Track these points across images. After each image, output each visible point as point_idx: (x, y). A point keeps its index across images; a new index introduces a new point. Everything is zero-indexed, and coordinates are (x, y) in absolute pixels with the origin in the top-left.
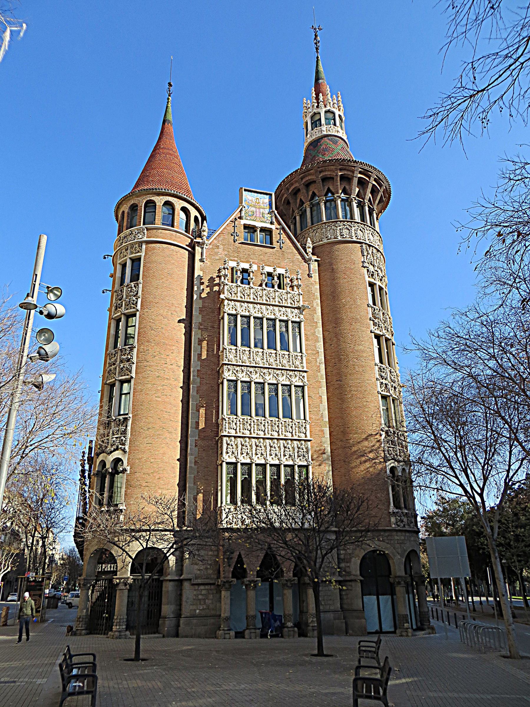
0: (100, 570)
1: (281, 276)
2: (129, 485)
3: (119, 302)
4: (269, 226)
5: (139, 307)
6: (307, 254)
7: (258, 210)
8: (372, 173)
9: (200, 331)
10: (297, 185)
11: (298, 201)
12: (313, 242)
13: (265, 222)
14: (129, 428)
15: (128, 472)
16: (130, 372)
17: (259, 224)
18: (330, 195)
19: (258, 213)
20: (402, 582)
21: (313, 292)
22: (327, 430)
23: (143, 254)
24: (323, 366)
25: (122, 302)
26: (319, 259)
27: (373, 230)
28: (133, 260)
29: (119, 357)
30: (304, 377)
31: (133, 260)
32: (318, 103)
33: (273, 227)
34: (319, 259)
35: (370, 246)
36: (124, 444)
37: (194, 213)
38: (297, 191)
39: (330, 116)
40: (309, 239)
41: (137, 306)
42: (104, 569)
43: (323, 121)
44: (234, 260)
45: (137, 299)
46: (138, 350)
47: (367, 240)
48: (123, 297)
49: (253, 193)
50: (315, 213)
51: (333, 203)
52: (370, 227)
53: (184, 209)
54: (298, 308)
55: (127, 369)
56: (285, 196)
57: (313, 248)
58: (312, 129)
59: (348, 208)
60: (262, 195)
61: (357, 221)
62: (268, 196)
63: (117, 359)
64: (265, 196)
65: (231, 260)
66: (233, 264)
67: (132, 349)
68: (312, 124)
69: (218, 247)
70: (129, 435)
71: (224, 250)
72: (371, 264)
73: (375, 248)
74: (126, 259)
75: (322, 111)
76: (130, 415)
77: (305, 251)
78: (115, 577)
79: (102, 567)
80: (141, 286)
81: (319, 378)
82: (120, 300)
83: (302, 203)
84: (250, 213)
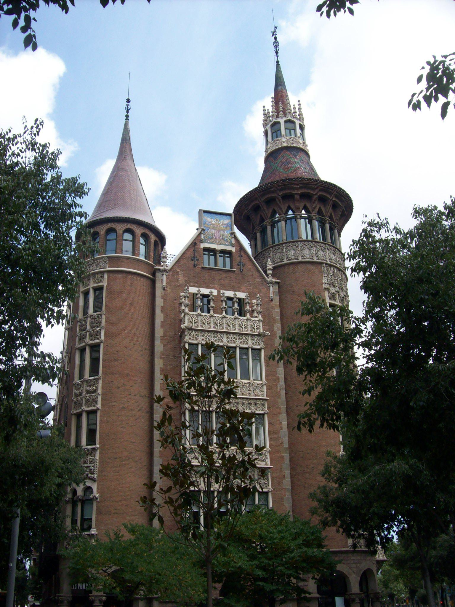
0: (76, 588)
1: (242, 300)
2: (99, 512)
3: (83, 333)
4: (229, 248)
5: (102, 337)
6: (267, 275)
7: (217, 232)
8: (332, 190)
10: (257, 202)
11: (259, 216)
12: (274, 262)
14: (97, 458)
15: (98, 500)
16: (96, 403)
18: (290, 212)
20: (357, 599)
21: (273, 316)
22: (287, 456)
23: (104, 284)
24: (283, 392)
25: (86, 333)
26: (280, 281)
27: (333, 249)
28: (95, 289)
29: (84, 389)
30: (263, 405)
31: (95, 289)
32: (278, 112)
33: (233, 250)
34: (280, 281)
35: (331, 266)
36: (93, 473)
37: (153, 238)
38: (257, 208)
39: (290, 125)
40: (269, 260)
41: (100, 337)
42: (80, 587)
43: (283, 132)
44: (194, 286)
45: (100, 330)
46: (103, 382)
47: (328, 260)
48: (87, 327)
49: (212, 215)
50: (275, 230)
51: (293, 220)
52: (331, 246)
53: (144, 235)
54: (259, 335)
55: (93, 400)
56: (246, 211)
57: (274, 268)
58: (273, 139)
59: (308, 226)
60: (222, 216)
61: (319, 240)
62: (228, 217)
63: (83, 390)
64: (225, 217)
65: (191, 286)
66: (193, 290)
67: (97, 380)
68: (272, 133)
69: (178, 273)
70: (98, 465)
72: (332, 285)
73: (336, 267)
74: (89, 289)
75: (282, 121)
76: (98, 446)
77: (265, 272)
78: (90, 594)
79: (77, 586)
80: (104, 317)
81: (280, 404)
82: (84, 330)
83: (262, 220)
84: (210, 236)
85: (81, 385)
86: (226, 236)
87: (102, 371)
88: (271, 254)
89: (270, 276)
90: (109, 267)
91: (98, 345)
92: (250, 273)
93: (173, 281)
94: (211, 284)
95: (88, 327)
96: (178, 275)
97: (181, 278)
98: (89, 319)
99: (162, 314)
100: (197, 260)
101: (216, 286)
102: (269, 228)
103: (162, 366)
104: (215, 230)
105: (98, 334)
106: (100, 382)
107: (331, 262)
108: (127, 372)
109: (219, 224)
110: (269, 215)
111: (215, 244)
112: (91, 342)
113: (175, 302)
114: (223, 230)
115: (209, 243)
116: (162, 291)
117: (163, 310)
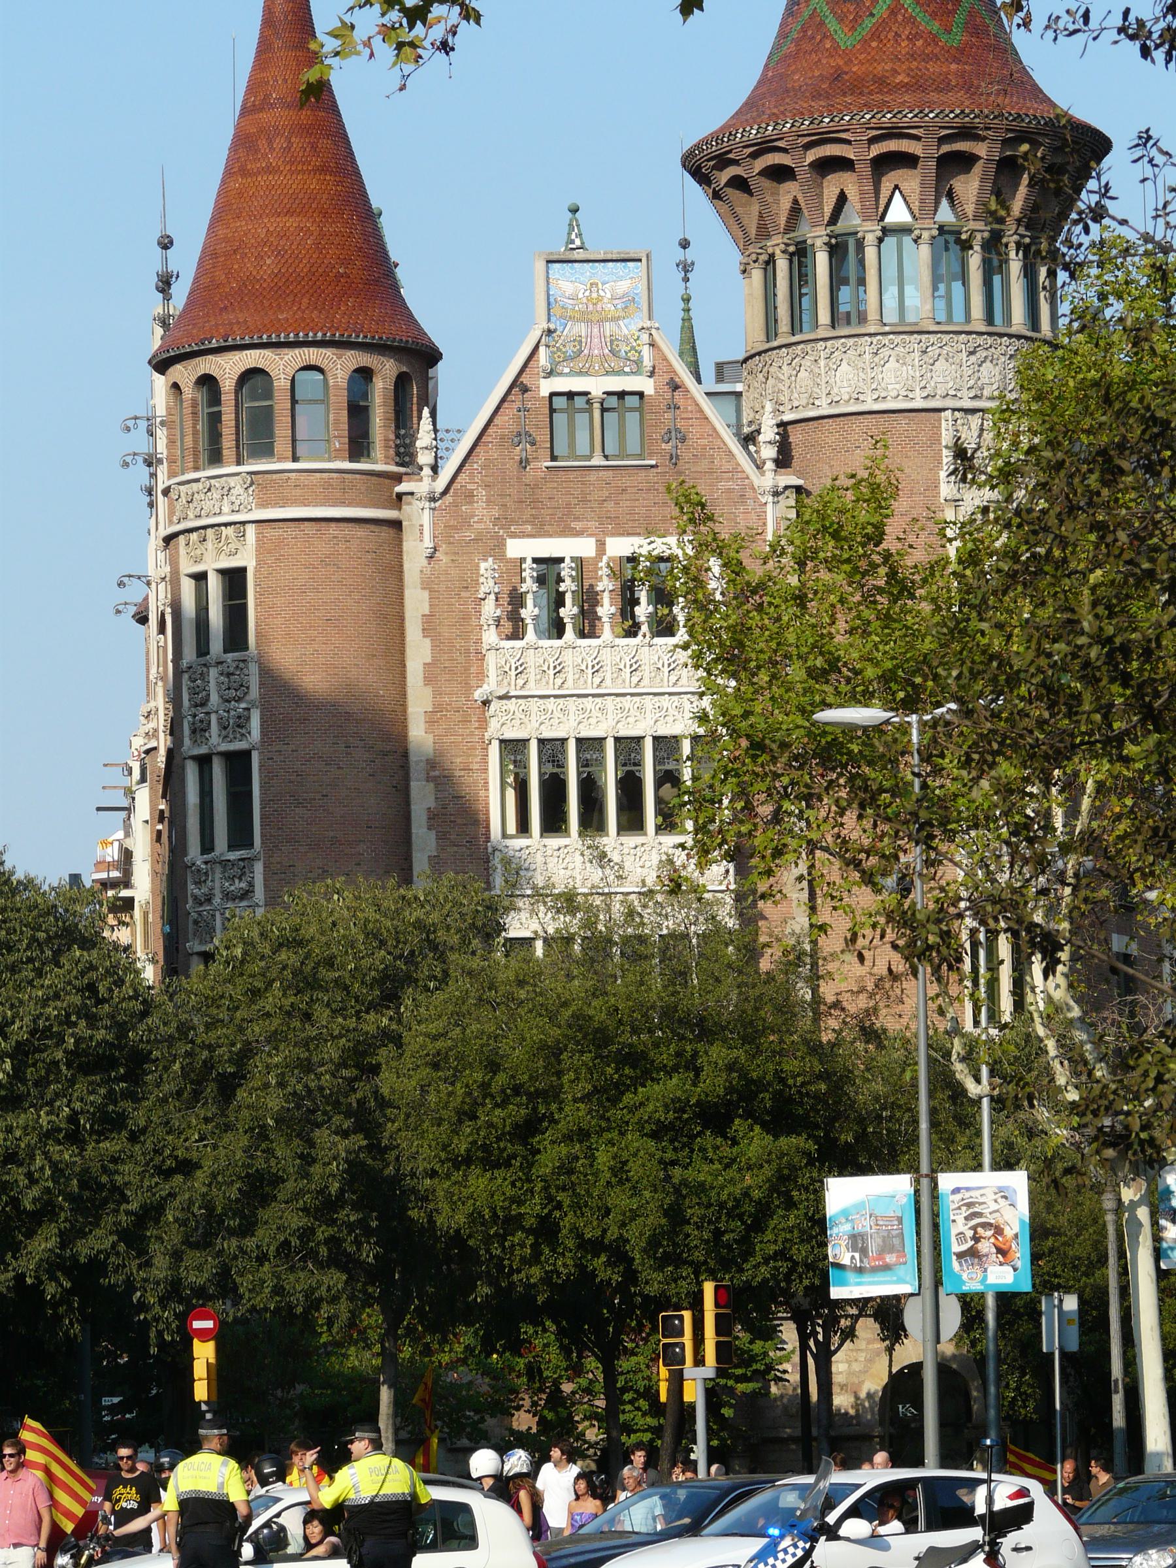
6: (759, 467)
9: (432, 785)
13: (619, 372)
17: (596, 386)
19: (596, 340)
25: (208, 713)
29: (217, 884)
33: (647, 385)
65: (514, 536)
66: (517, 548)
69: (470, 496)
71: (488, 501)
83: (764, 232)
84: (570, 350)
85: (206, 874)
86: (626, 340)
87: (262, 835)
88: (785, 367)
89: (770, 465)
90: (263, 505)
91: (246, 755)
92: (703, 465)
93: (454, 528)
94: (577, 519)
95: (214, 698)
96: (471, 503)
97: (482, 512)
98: (213, 673)
99: (428, 641)
100: (533, 444)
101: (593, 524)
102: (782, 264)
103: (432, 805)
104: (589, 322)
105: (242, 722)
106: (259, 867)
107: (975, 397)
108: (332, 834)
109: (600, 299)
110: (783, 220)
111: (587, 374)
112: (225, 747)
113: (463, 594)
114: (615, 319)
115: (567, 375)
116: (425, 562)
117: (429, 627)
